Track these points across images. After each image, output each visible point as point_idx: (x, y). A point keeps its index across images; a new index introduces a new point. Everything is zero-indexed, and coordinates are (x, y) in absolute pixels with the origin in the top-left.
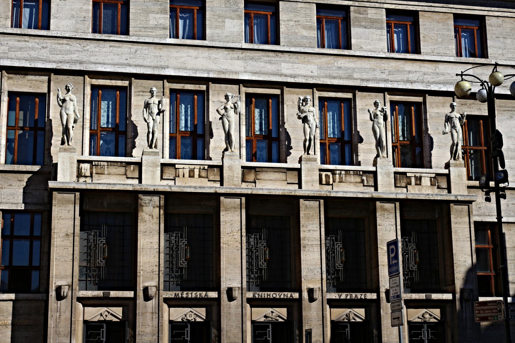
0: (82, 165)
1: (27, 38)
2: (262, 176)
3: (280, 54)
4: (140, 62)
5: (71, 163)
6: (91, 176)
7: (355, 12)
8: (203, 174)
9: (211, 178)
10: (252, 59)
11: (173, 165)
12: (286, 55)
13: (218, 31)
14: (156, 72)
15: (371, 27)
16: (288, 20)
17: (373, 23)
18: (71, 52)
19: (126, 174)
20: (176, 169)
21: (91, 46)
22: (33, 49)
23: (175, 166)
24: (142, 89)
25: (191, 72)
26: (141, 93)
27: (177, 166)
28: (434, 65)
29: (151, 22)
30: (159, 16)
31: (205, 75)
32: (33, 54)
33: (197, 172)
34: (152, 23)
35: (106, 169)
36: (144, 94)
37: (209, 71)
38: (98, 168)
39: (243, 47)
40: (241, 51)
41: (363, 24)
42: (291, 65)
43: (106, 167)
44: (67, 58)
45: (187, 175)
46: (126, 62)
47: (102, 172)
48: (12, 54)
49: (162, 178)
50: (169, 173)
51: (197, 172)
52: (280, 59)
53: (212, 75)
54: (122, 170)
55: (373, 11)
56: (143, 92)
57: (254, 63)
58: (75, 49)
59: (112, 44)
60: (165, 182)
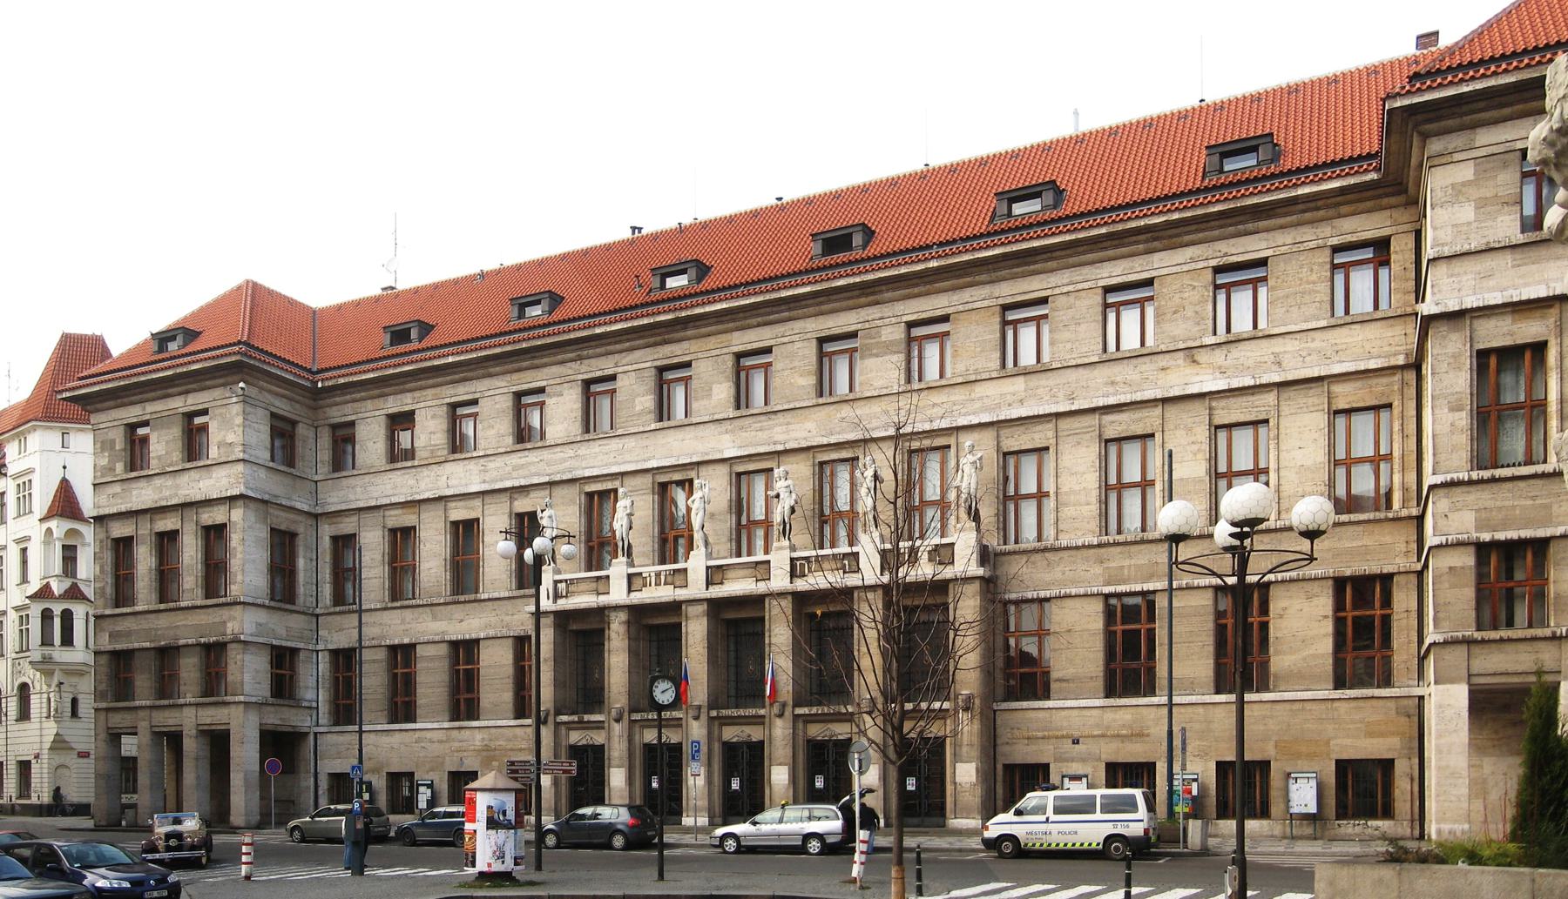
0: (559, 585)
1: (526, 453)
2: (730, 574)
3: (773, 417)
4: (628, 457)
7: (865, 337)
8: (670, 579)
9: (677, 584)
11: (641, 574)
12: (780, 415)
13: (705, 402)
14: (640, 467)
15: (886, 354)
17: (888, 348)
18: (565, 460)
19: (597, 590)
21: (583, 450)
22: (533, 463)
27: (644, 575)
28: (969, 387)
29: (637, 408)
30: (645, 398)
31: (688, 461)
32: (533, 469)
33: (663, 578)
34: (638, 408)
37: (691, 456)
40: (729, 422)
41: (875, 351)
44: (561, 467)
45: (653, 583)
46: (614, 460)
48: (515, 474)
49: (630, 591)
50: (637, 582)
51: (663, 578)
54: (594, 585)
55: (889, 329)
57: (744, 434)
58: (567, 455)
59: (600, 442)
60: (633, 595)
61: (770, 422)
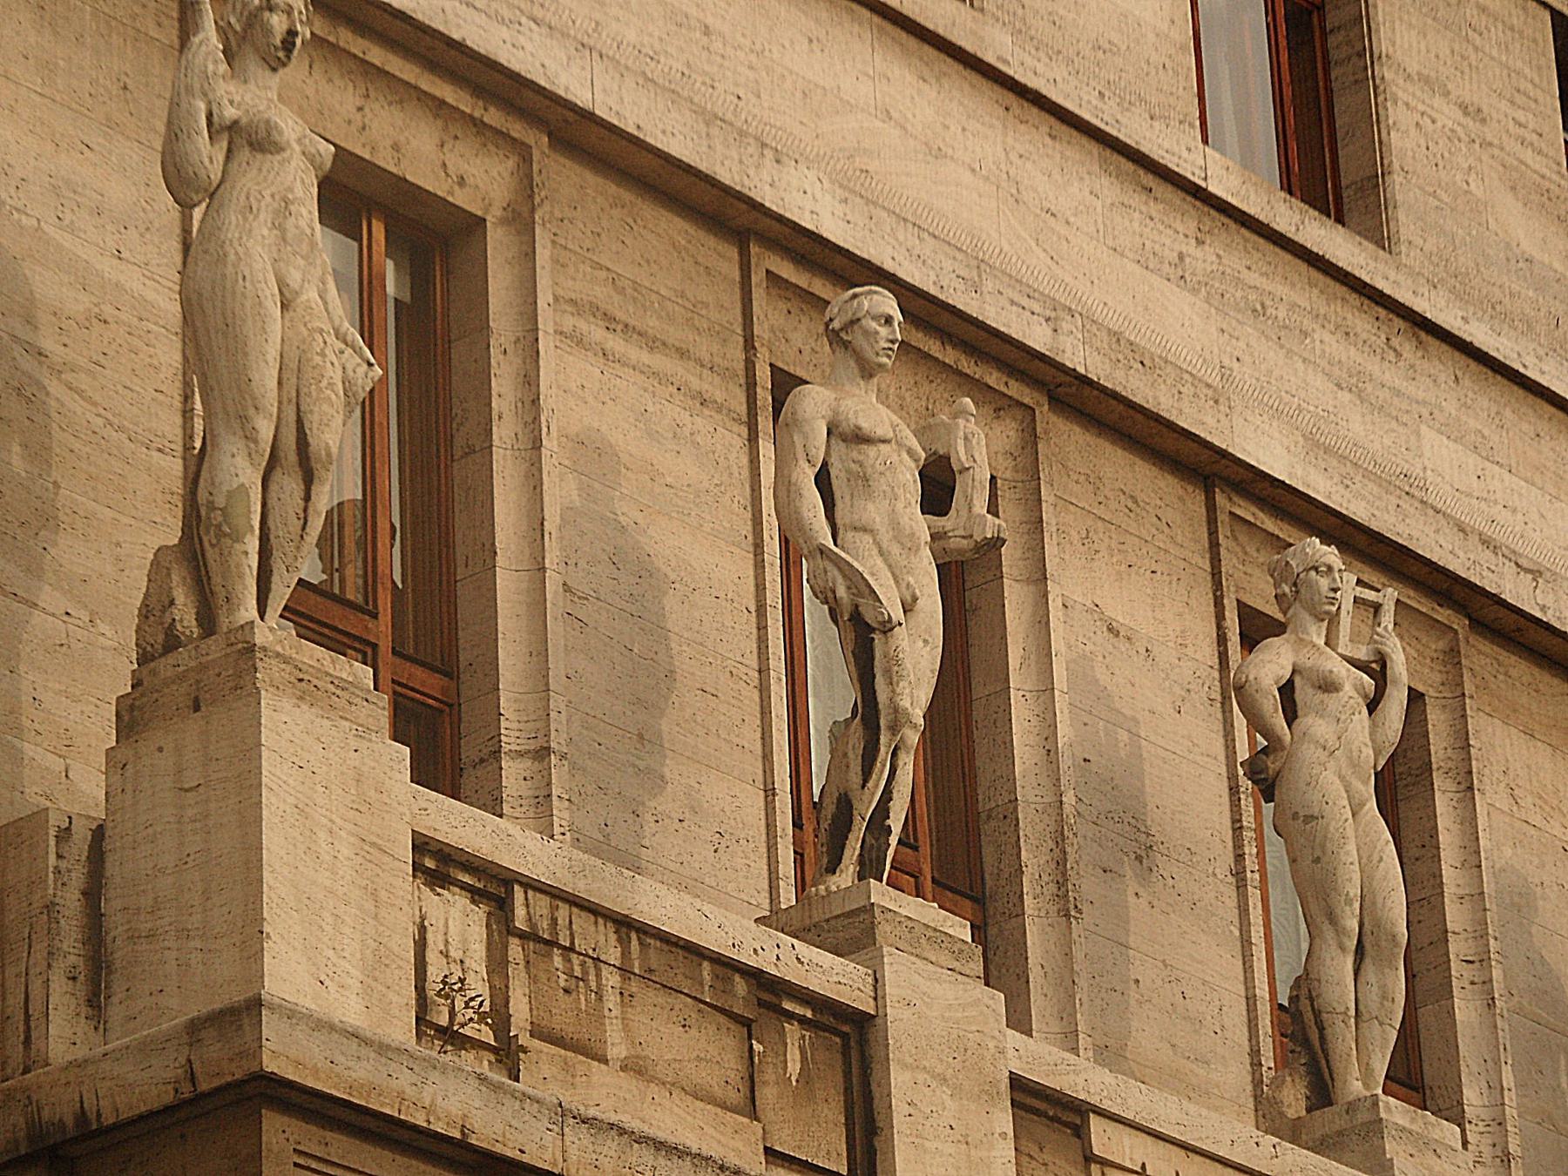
5: (371, 848)
6: (507, 1054)
10: (1260, 312)
12: (1441, 366)
16: (1425, 80)
20: (1089, 1158)
23: (1080, 1132)
24: (601, 293)
25: (948, 265)
26: (596, 332)
31: (1037, 337)
35: (612, 1000)
36: (615, 343)
38: (551, 976)
39: (1213, 188)
42: (1472, 460)
43: (611, 979)
47: (585, 1035)
52: (1409, 388)
53: (1077, 355)
56: (609, 320)
61: (1392, 376)
